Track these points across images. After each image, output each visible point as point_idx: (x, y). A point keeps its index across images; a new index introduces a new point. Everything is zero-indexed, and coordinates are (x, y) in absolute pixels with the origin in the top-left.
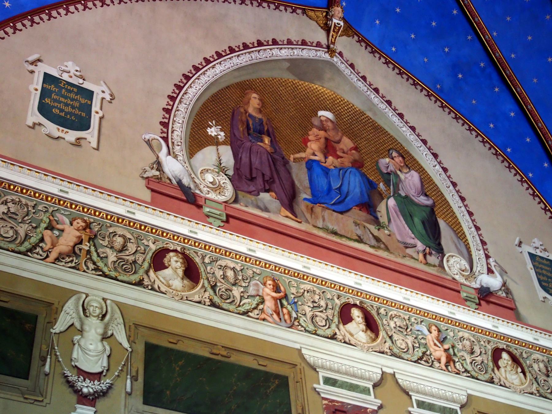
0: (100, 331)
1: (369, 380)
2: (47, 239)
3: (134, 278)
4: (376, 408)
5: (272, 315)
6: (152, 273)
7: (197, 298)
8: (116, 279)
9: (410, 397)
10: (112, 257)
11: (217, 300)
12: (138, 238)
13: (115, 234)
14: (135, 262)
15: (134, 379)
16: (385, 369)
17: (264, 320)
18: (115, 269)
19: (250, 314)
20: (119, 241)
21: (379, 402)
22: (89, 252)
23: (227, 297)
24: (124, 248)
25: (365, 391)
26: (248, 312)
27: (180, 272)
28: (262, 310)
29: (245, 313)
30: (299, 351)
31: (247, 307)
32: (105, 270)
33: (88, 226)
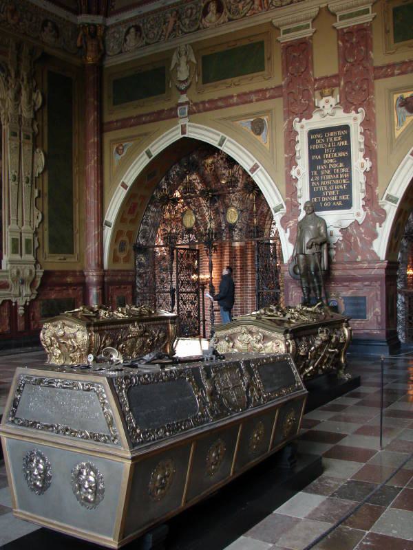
0: (185, 60)
1: (307, 19)
2: (164, 30)
3: (196, 27)
4: (311, 35)
5: (258, 9)
6: (203, 20)
7: (222, 21)
8: (190, 32)
9: (336, 16)
10: (187, 21)
11: (231, 16)
12: (197, 5)
13: (188, 9)
14: (196, 19)
15: (199, 75)
16: (322, 6)
17: (254, 13)
18: (189, 28)
19: (247, 15)
20: (190, 11)
21: (314, 29)
22: (179, 26)
23: (237, 12)
24: (192, 13)
25: (307, 26)
26: (246, 14)
27: (215, 12)
28: (253, 9)
29: (245, 16)
30: (271, 22)
31: (245, 12)
32: (185, 31)
33: (177, 12)
